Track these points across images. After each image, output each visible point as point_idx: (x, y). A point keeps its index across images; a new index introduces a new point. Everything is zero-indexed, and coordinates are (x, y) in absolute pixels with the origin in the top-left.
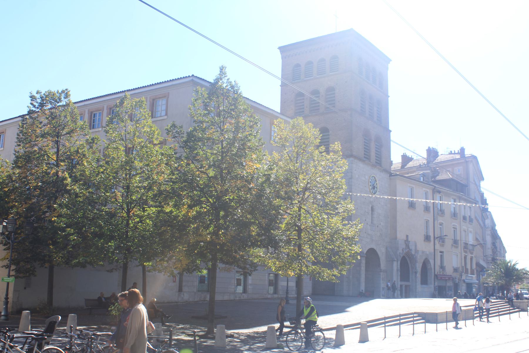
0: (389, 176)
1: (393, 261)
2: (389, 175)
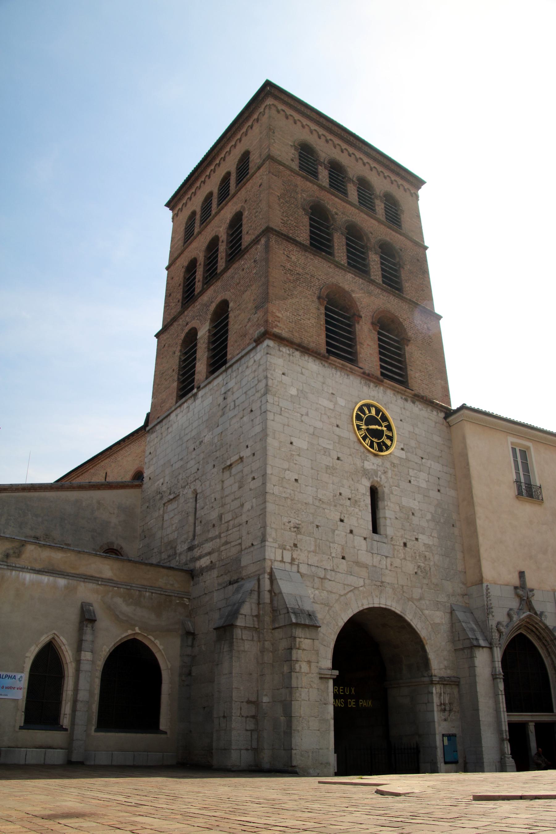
0: (445, 418)
1: (474, 647)
2: (442, 415)
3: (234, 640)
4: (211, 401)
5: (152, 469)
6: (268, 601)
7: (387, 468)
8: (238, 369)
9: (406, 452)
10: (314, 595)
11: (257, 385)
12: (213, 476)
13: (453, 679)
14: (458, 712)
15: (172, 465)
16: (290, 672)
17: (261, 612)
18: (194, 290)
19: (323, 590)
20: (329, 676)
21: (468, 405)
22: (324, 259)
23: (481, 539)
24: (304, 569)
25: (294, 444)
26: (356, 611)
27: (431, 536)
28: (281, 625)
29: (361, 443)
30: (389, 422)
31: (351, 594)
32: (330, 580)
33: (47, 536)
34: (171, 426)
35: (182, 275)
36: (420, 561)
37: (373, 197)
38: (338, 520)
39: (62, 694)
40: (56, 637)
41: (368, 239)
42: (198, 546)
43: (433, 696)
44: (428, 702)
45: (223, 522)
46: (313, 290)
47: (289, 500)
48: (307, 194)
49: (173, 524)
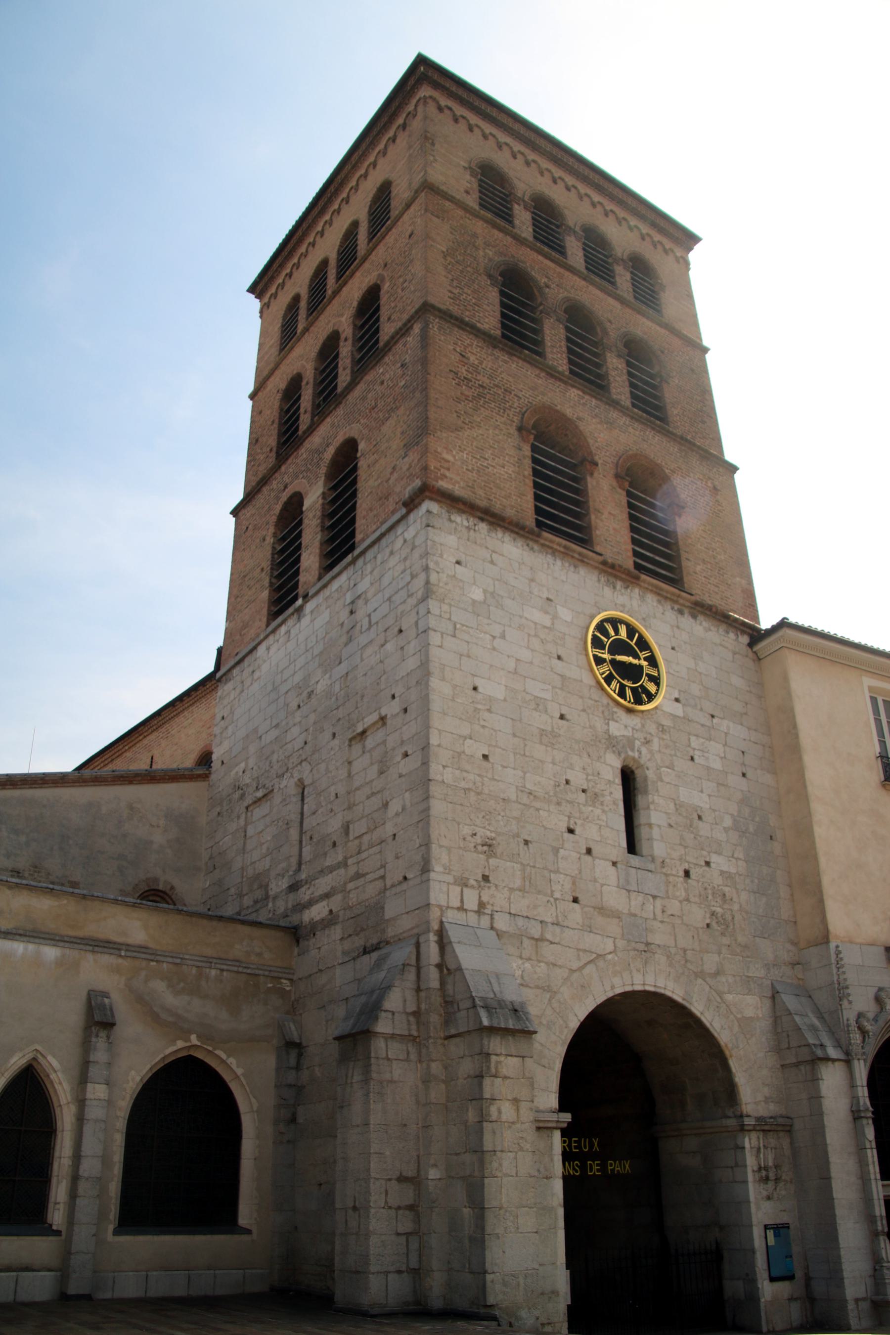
0: (751, 645)
1: (817, 1060)
2: (745, 639)
3: (373, 1061)
4: (327, 619)
5: (226, 745)
6: (435, 984)
7: (650, 734)
8: (375, 558)
9: (684, 705)
10: (523, 971)
11: (409, 583)
12: (332, 753)
13: (781, 1121)
14: (791, 1182)
15: (261, 737)
16: (479, 1122)
17: (423, 1006)
18: (297, 429)
19: (539, 961)
20: (554, 1125)
21: (793, 620)
22: (529, 362)
23: (823, 861)
24: (502, 923)
25: (480, 689)
26: (601, 999)
27: (733, 856)
28: (461, 1030)
29: (603, 689)
30: (651, 651)
31: (590, 969)
32: (552, 943)
33: (36, 868)
34: (259, 667)
35: (277, 404)
37: (610, 260)
38: (564, 829)
39: (52, 1163)
40: (39, 1056)
41: (605, 332)
42: (306, 883)
43: (745, 1155)
44: (737, 1165)
45: (351, 838)
46: (508, 415)
47: (472, 794)
48: (493, 250)
49: (263, 844)
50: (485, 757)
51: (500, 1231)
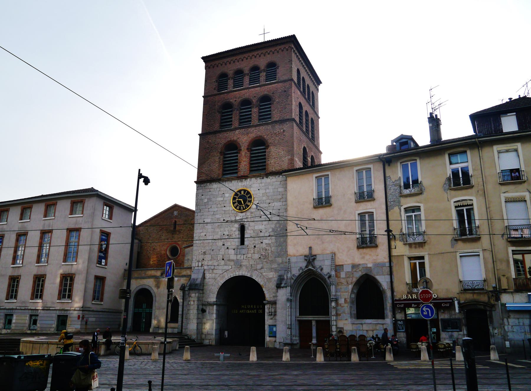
31: (226, 273)
36: (263, 252)
50: (205, 235)
51: (190, 323)
